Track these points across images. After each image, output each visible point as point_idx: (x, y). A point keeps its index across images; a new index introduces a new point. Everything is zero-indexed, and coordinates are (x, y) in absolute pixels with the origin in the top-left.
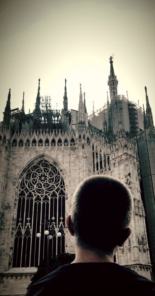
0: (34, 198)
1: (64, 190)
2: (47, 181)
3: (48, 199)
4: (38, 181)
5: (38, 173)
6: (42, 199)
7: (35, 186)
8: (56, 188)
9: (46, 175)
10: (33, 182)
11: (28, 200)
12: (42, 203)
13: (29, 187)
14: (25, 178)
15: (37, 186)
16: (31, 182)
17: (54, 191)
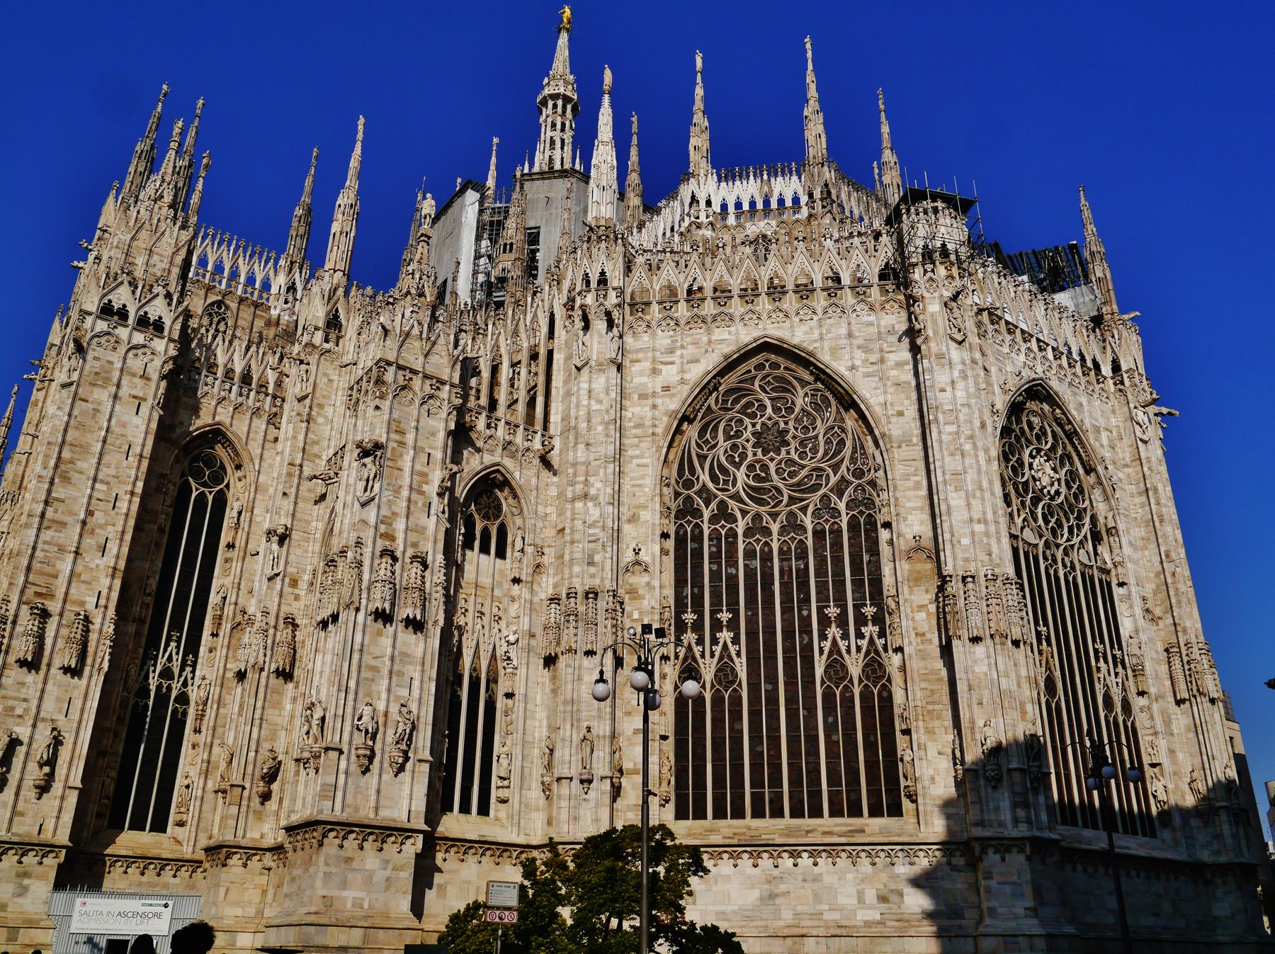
0: (740, 528)
1: (868, 488)
2: (788, 453)
3: (802, 528)
4: (750, 454)
5: (747, 421)
6: (775, 528)
7: (741, 474)
8: (834, 480)
9: (782, 425)
10: (730, 459)
11: (715, 536)
12: (775, 546)
13: (714, 478)
14: (693, 444)
15: (748, 476)
16: (723, 459)
17: (825, 495)
